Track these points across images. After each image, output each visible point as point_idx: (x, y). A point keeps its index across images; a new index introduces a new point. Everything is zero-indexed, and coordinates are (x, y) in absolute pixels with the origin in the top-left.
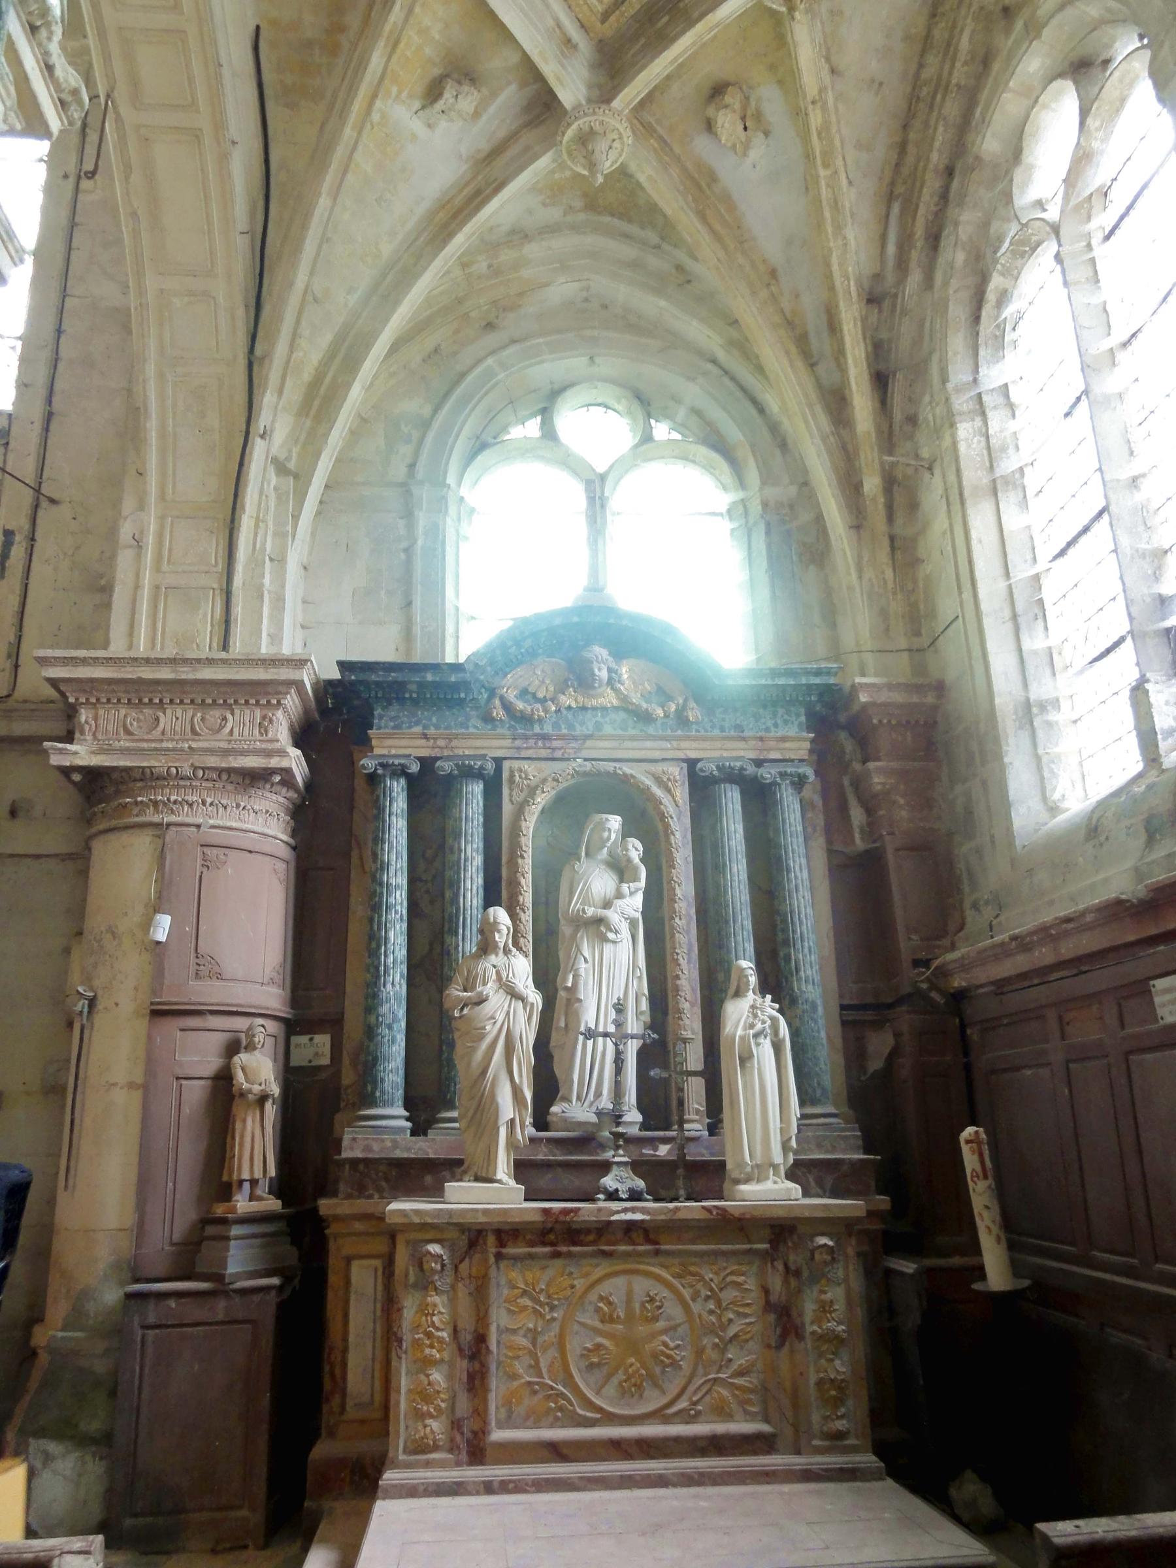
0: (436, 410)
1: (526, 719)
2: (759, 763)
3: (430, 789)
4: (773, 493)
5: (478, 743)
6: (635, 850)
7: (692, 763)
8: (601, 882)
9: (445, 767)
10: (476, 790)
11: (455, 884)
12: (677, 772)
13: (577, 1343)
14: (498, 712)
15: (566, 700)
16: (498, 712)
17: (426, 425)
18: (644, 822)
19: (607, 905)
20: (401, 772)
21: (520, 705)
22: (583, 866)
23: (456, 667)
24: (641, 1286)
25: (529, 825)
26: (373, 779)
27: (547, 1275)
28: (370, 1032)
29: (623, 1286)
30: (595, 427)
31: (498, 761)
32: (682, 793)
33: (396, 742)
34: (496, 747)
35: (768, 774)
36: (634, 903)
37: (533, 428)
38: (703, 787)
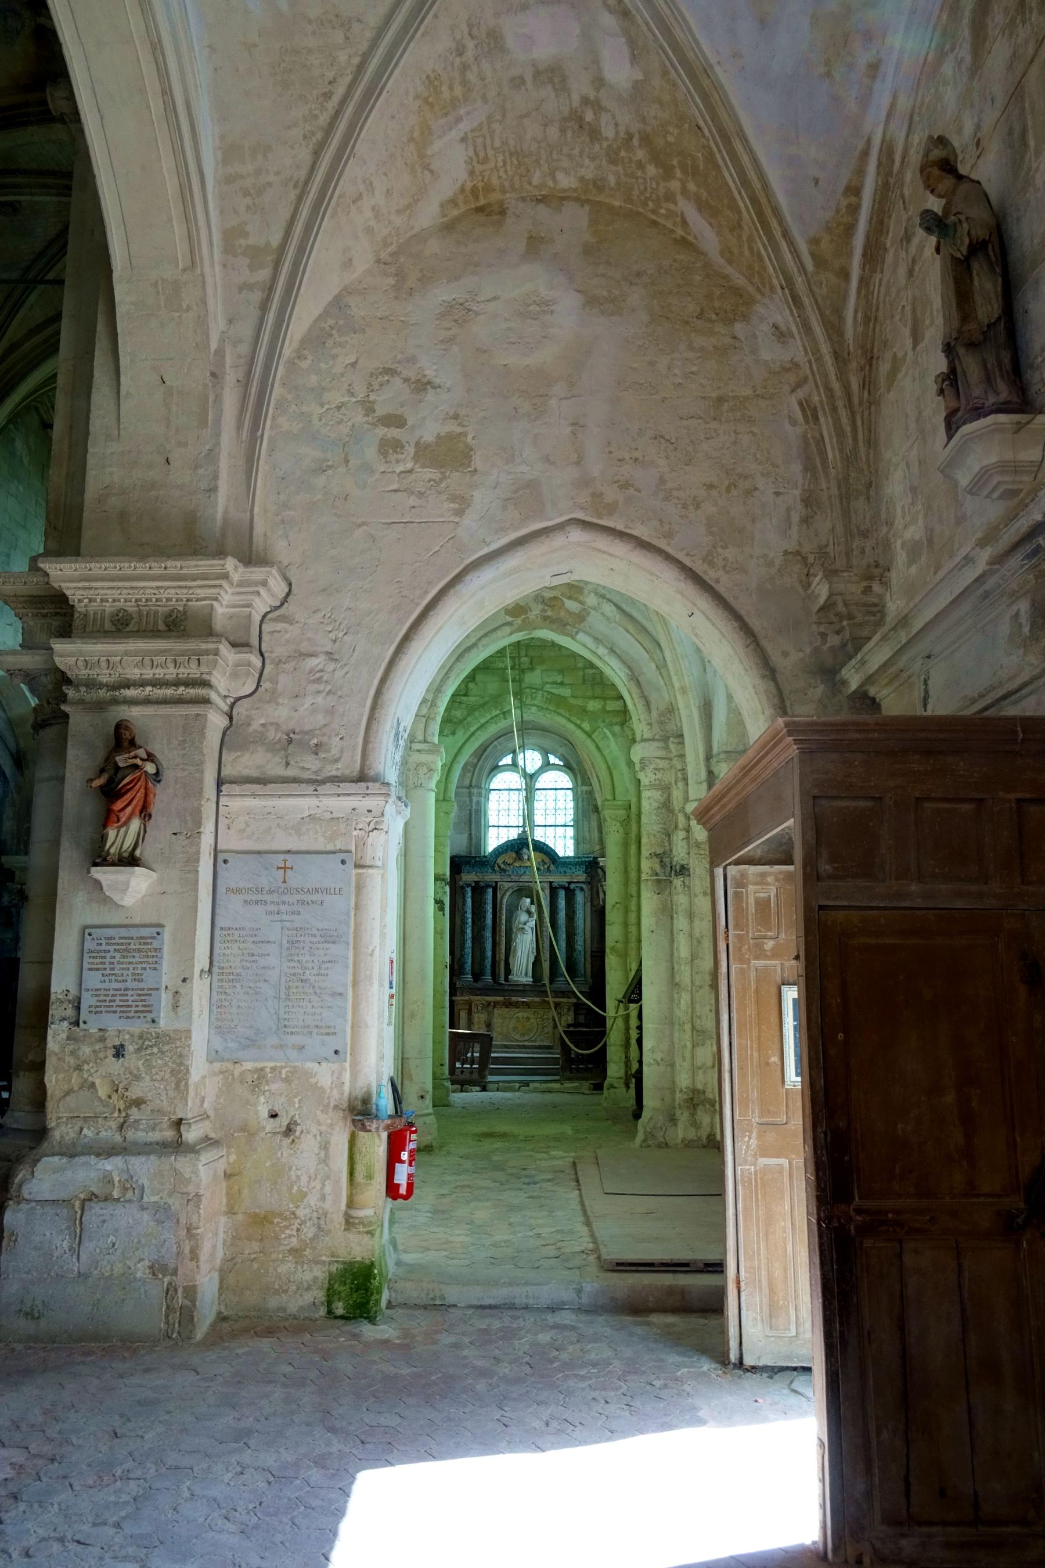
0: (479, 761)
1: (504, 871)
2: (570, 883)
3: (478, 890)
4: (585, 788)
5: (491, 877)
6: (533, 909)
7: (551, 883)
8: (524, 917)
9: (482, 884)
10: (490, 890)
11: (485, 917)
12: (547, 886)
13: (511, 1026)
14: (497, 868)
15: (516, 864)
16: (497, 868)
17: (475, 766)
18: (536, 901)
19: (525, 924)
20: (468, 885)
21: (503, 866)
22: (519, 912)
23: (485, 857)
24: (526, 1015)
25: (505, 901)
26: (462, 888)
27: (505, 1011)
28: (462, 956)
29: (521, 1014)
30: (532, 759)
31: (496, 883)
32: (548, 892)
33: (469, 877)
34: (496, 877)
35: (572, 886)
36: (532, 923)
37: (507, 760)
38: (553, 890)
